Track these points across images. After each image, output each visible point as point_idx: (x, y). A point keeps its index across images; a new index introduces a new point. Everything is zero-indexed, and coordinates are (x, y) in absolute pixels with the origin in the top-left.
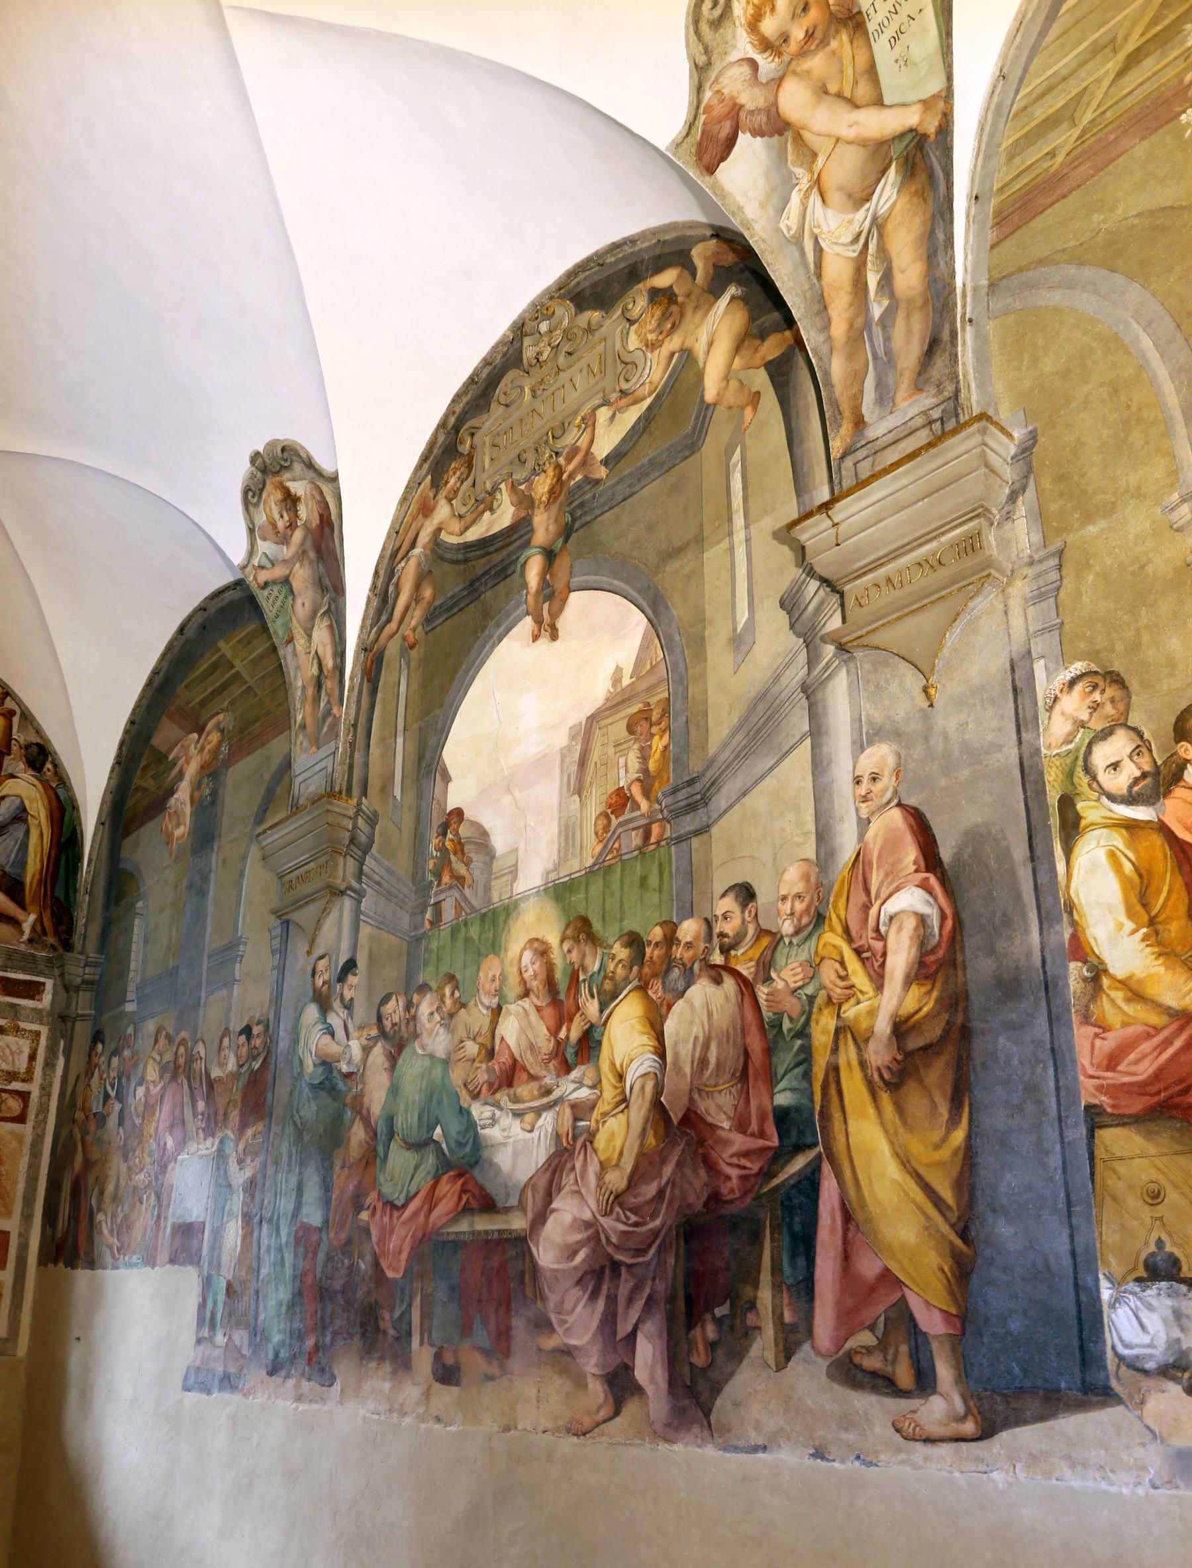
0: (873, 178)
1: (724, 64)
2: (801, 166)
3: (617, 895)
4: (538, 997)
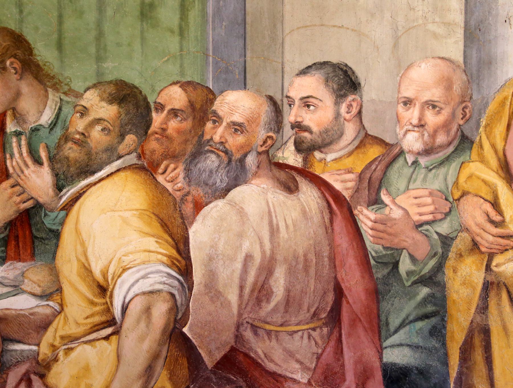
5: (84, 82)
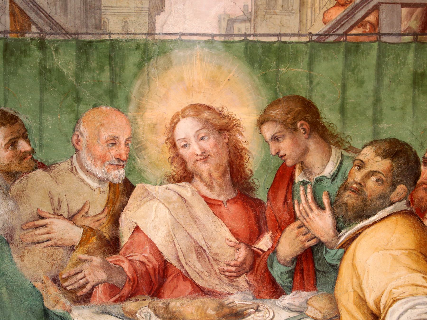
3: (370, 86)
4: (210, 187)
5: (362, 140)
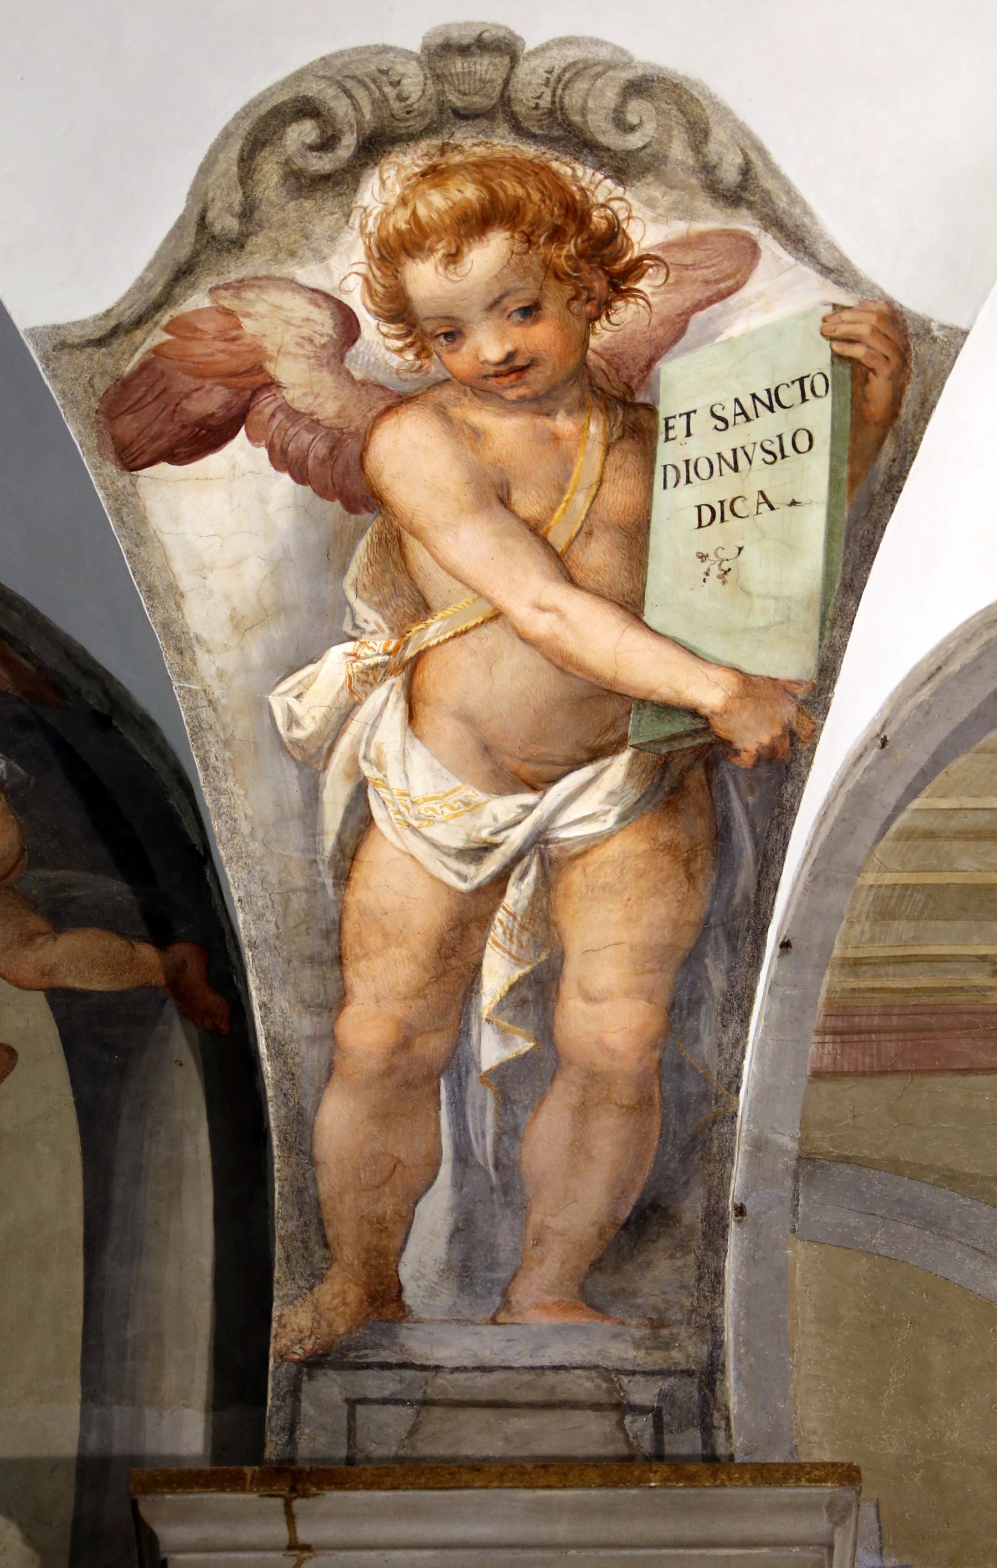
0: (562, 750)
1: (276, 271)
2: (380, 607)
